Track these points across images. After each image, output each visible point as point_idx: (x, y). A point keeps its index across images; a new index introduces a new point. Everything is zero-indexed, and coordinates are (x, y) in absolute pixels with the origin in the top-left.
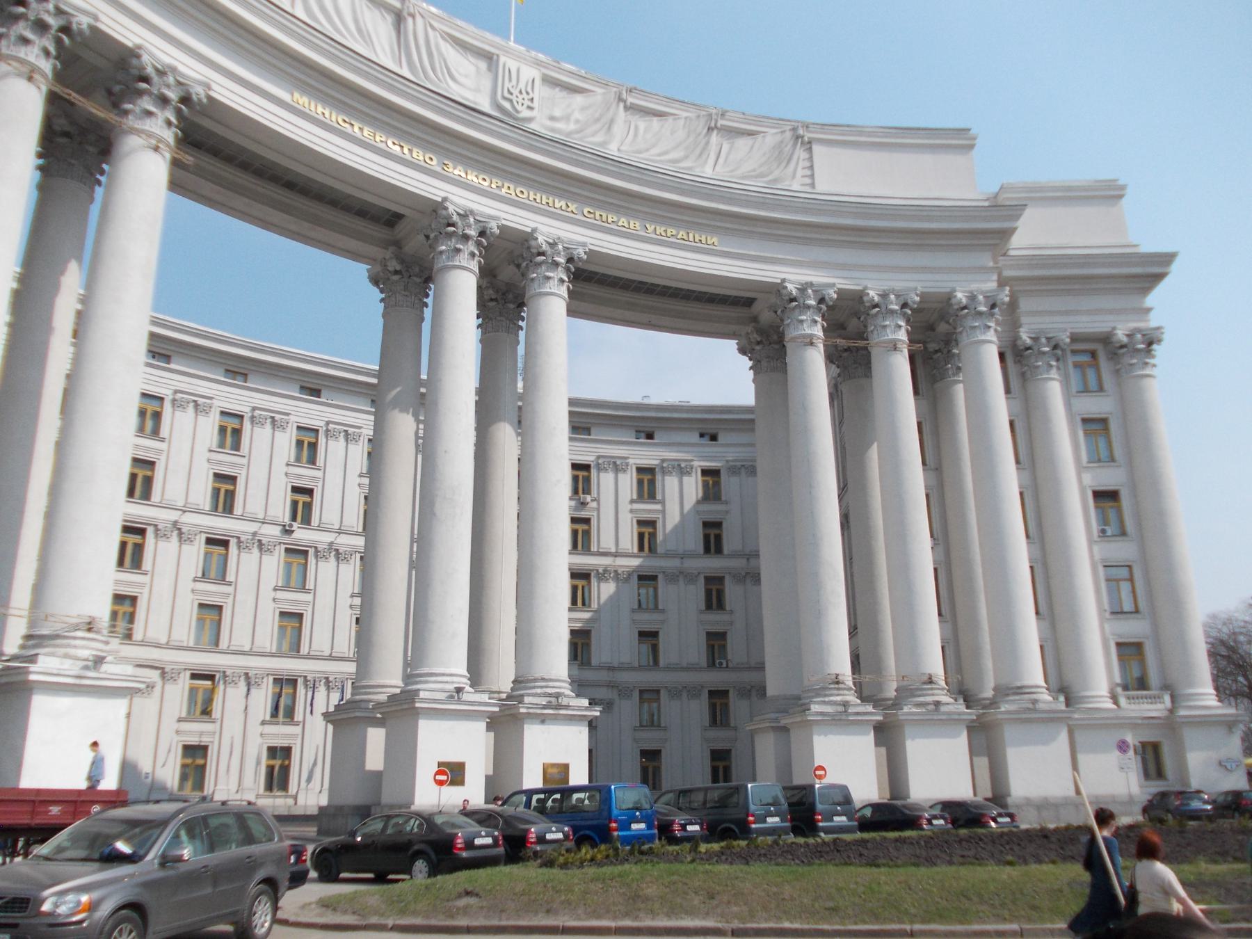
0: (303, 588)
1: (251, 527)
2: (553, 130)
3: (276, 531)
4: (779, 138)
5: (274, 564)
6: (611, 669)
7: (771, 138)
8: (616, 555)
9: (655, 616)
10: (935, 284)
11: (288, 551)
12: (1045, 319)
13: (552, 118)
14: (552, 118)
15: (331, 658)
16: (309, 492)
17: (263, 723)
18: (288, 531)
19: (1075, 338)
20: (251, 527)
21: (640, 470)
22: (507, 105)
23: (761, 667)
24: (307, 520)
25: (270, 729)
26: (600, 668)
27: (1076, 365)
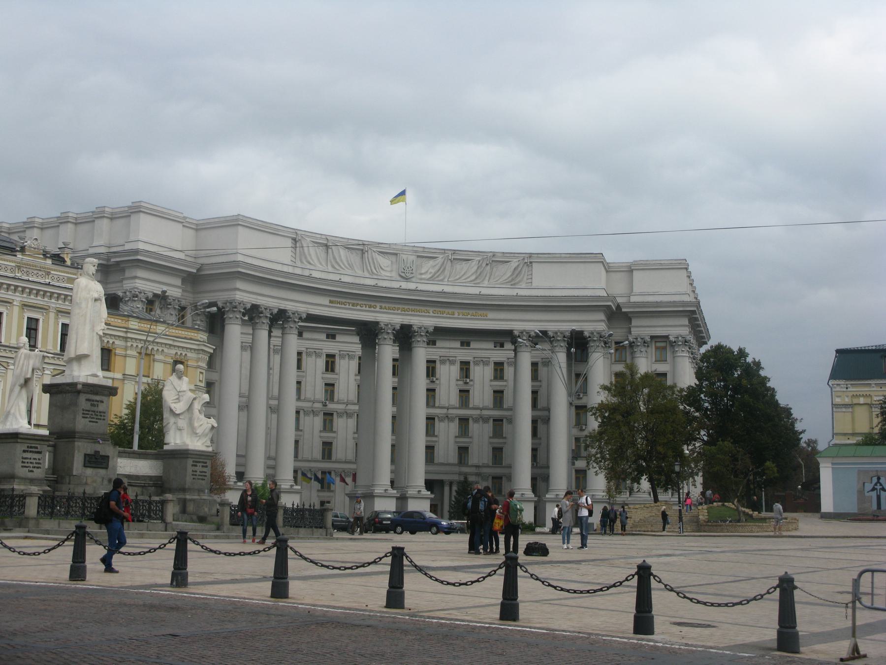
0: (331, 430)
1: (309, 404)
2: (421, 279)
3: (318, 406)
4: (517, 264)
5: (318, 421)
6: (477, 467)
7: (514, 264)
8: (481, 409)
9: (501, 441)
10: (576, 327)
11: (325, 414)
12: (642, 329)
13: (421, 274)
14: (421, 274)
15: (346, 462)
16: (333, 385)
17: (318, 491)
18: (325, 405)
19: (652, 337)
20: (309, 404)
21: (496, 364)
22: (403, 275)
23: (548, 467)
24: (332, 399)
25: (321, 494)
26: (472, 466)
27: (657, 348)
